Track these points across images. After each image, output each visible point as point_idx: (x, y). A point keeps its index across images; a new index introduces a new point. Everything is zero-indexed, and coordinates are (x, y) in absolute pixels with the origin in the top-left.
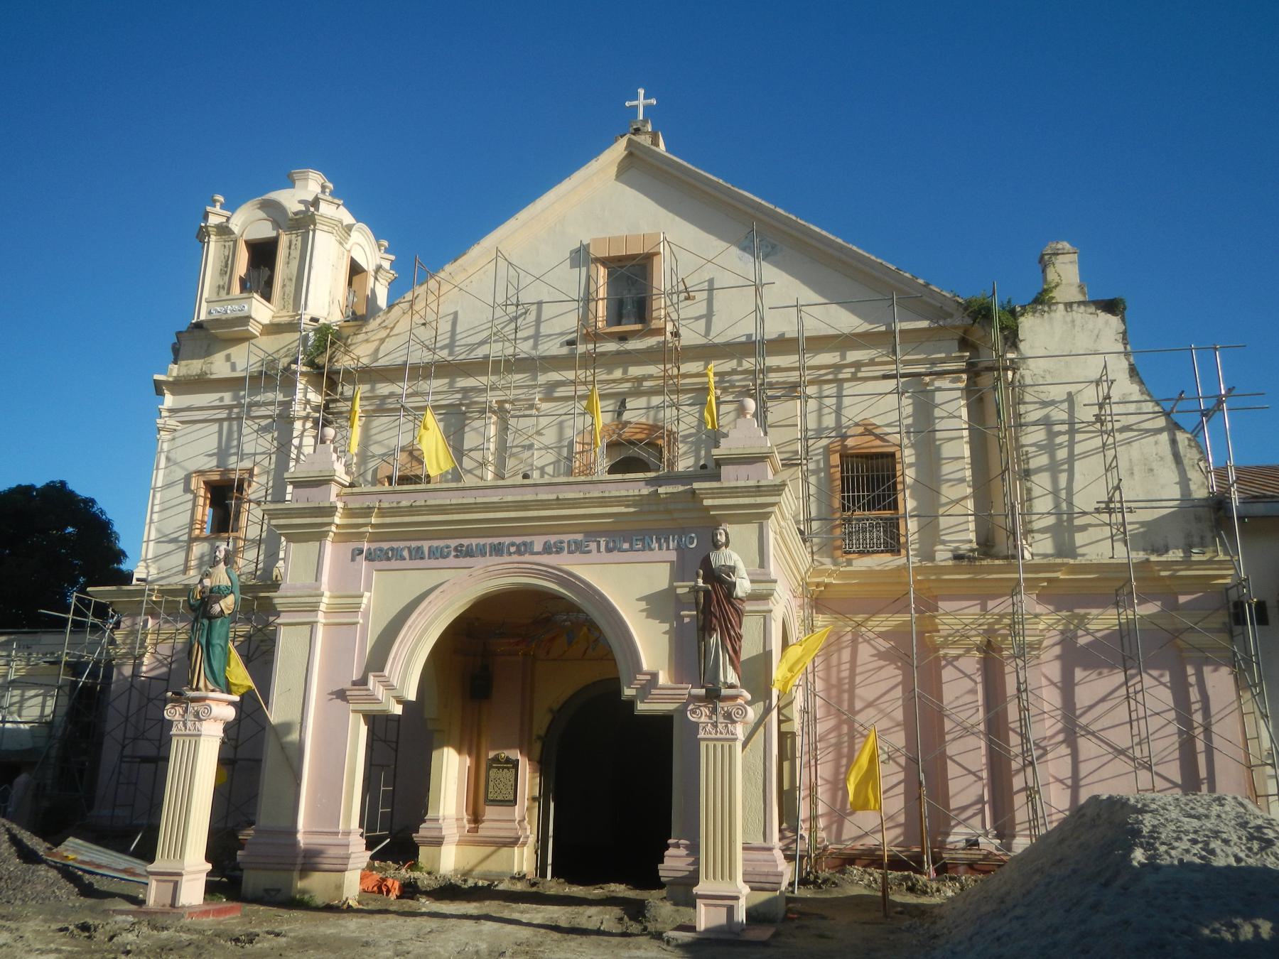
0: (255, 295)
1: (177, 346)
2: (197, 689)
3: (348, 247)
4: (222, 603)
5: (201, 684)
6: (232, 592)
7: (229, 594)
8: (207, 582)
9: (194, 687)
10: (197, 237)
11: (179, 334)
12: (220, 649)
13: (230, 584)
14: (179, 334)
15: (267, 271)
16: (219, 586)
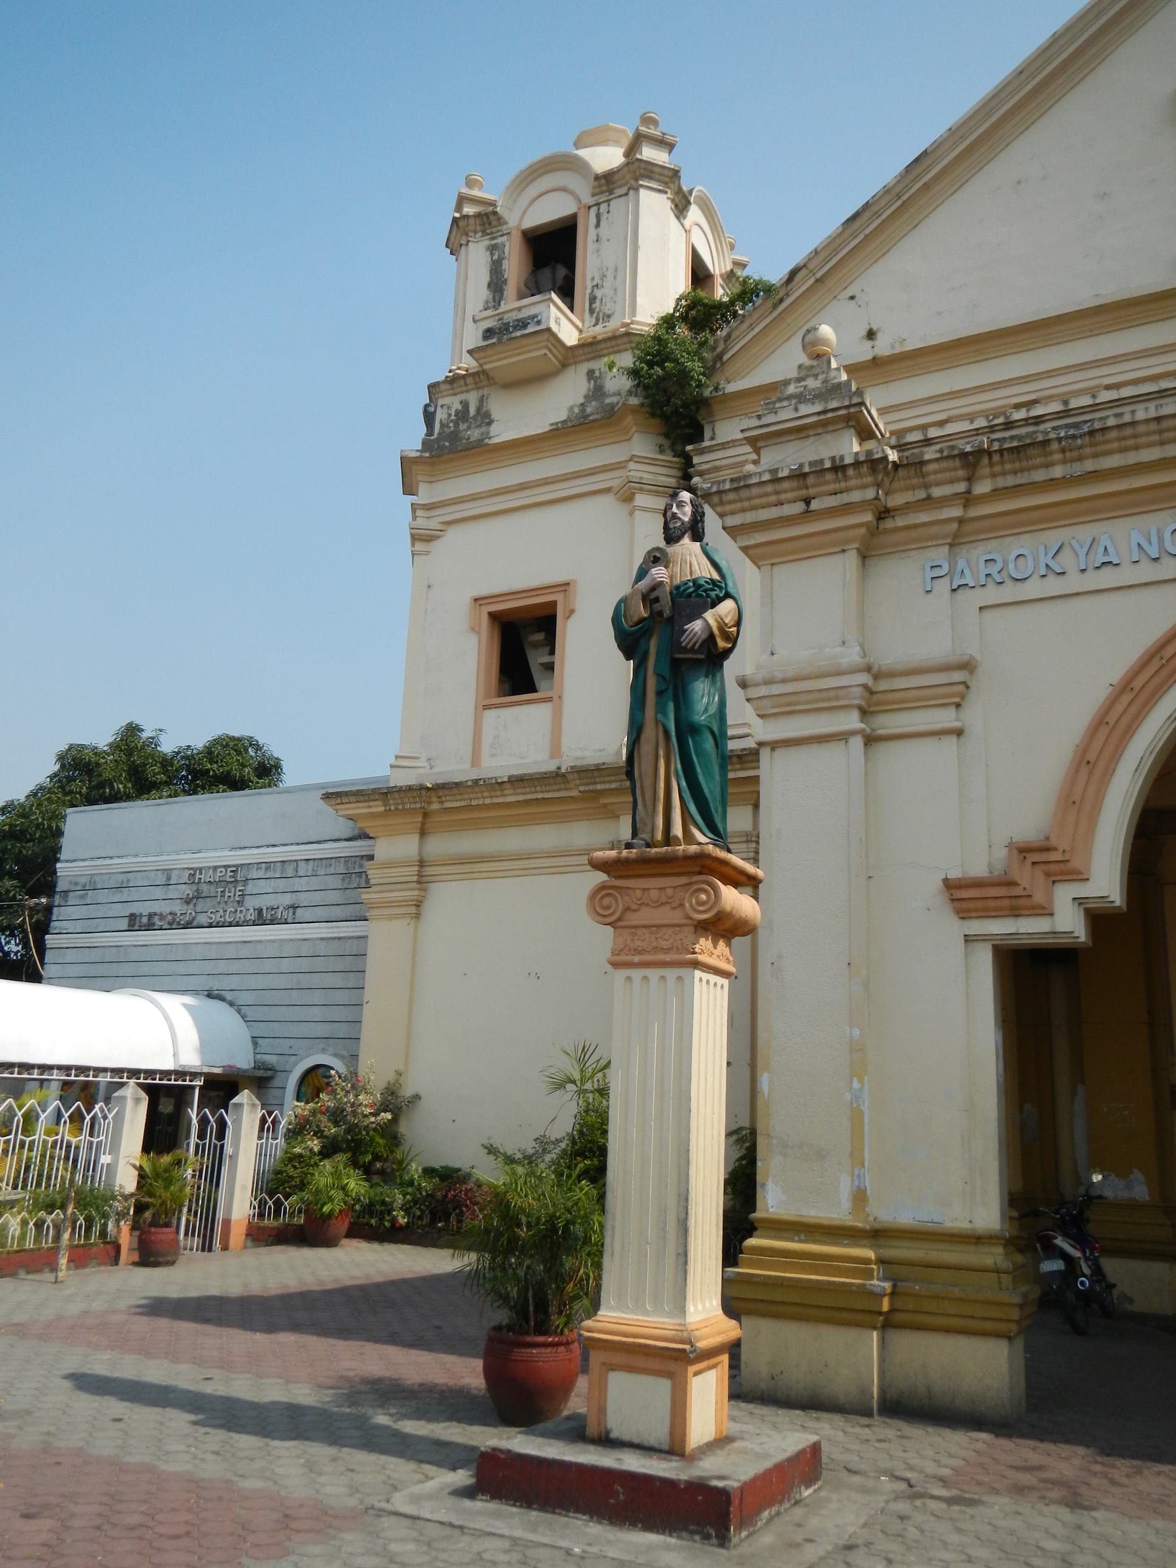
0: (554, 296)
1: (432, 409)
2: (668, 839)
3: (687, 222)
4: (710, 616)
5: (677, 830)
6: (728, 596)
7: (720, 600)
8: (659, 573)
9: (659, 836)
10: (447, 246)
11: (433, 388)
12: (711, 740)
13: (716, 576)
14: (433, 388)
15: (562, 272)
16: (694, 581)
